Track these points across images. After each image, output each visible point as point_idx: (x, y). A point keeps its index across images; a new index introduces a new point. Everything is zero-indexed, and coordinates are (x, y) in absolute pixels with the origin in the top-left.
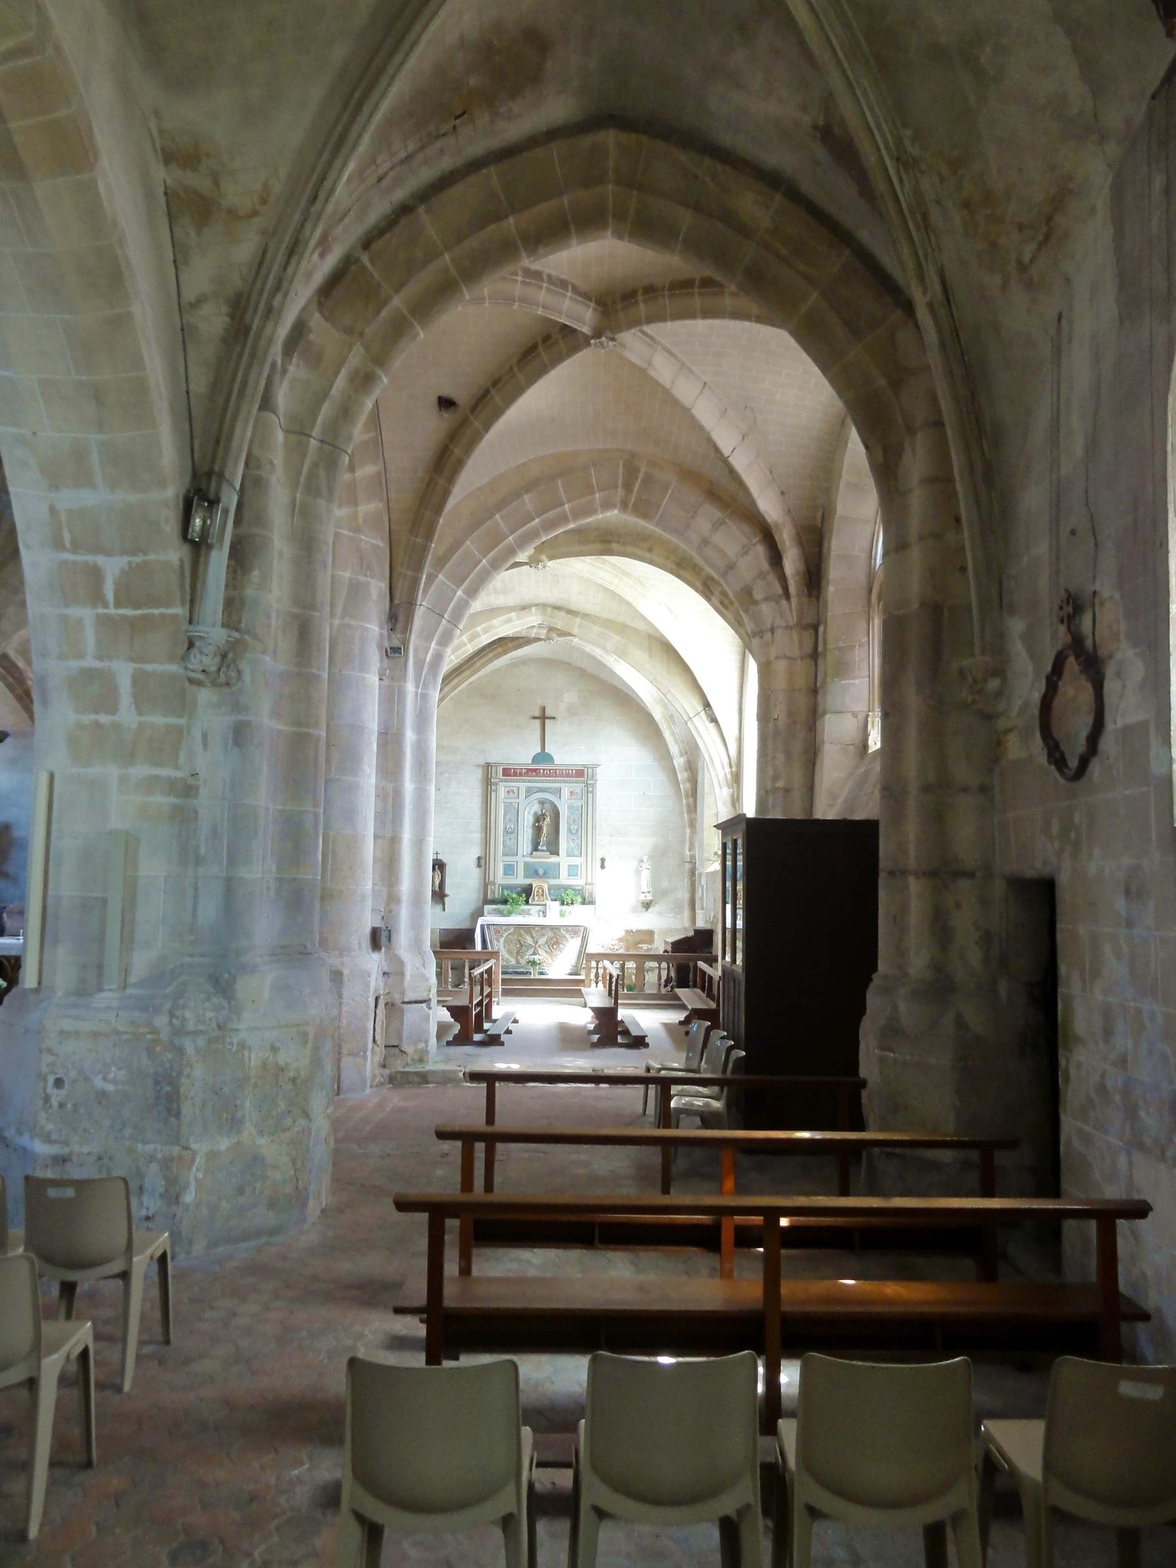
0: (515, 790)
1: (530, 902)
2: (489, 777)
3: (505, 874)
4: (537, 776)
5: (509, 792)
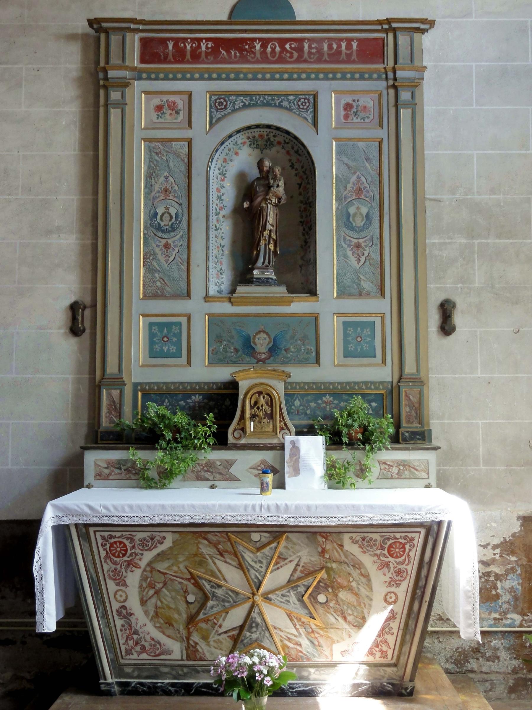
0: (181, 102)
1: (231, 439)
2: (102, 64)
3: (153, 354)
4: (244, 60)
5: (159, 108)
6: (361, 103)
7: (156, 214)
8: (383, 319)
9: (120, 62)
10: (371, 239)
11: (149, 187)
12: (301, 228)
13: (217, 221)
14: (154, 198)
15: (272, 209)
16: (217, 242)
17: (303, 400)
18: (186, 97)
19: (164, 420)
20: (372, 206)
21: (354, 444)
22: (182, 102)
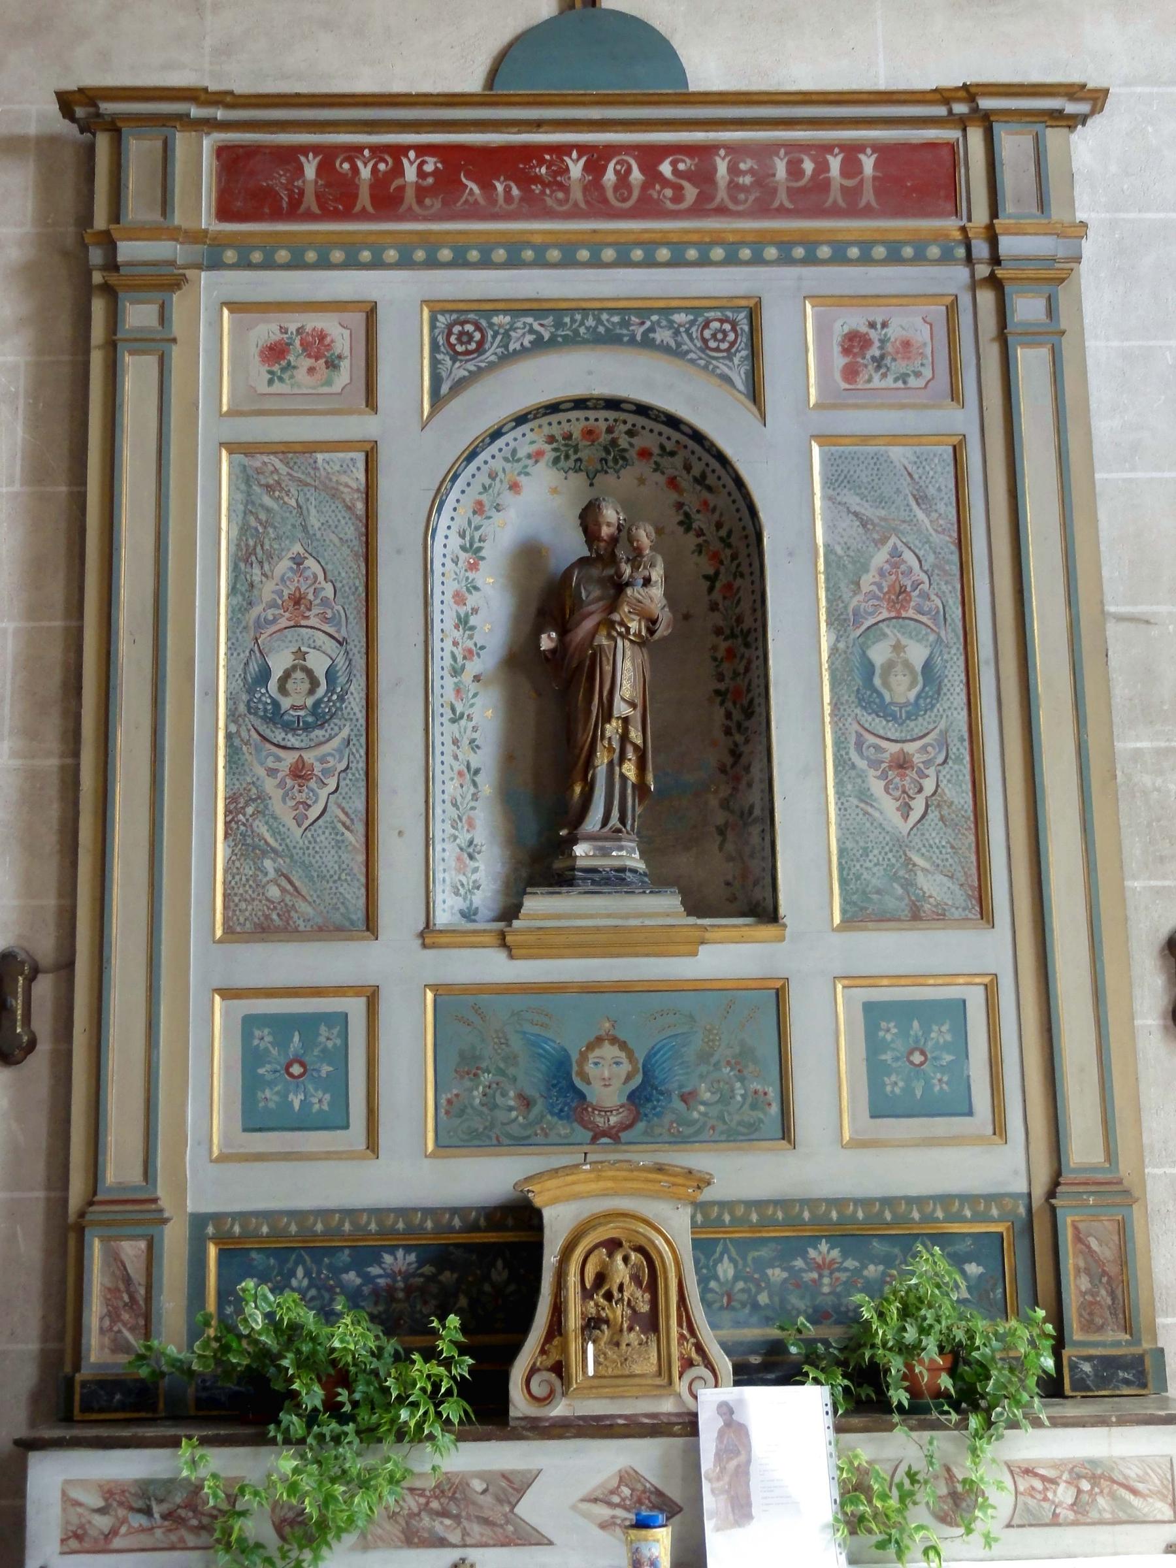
1: (519, 1404)
2: (100, 221)
4: (534, 208)
5: (275, 353)
6: (893, 332)
7: (264, 674)
8: (991, 991)
9: (156, 216)
10: (944, 742)
11: (244, 590)
12: (719, 714)
13: (458, 691)
14: (260, 625)
15: (628, 653)
16: (456, 757)
17: (744, 1258)
18: (359, 318)
19: (297, 1344)
20: (939, 639)
21: (926, 1410)
22: (347, 333)
